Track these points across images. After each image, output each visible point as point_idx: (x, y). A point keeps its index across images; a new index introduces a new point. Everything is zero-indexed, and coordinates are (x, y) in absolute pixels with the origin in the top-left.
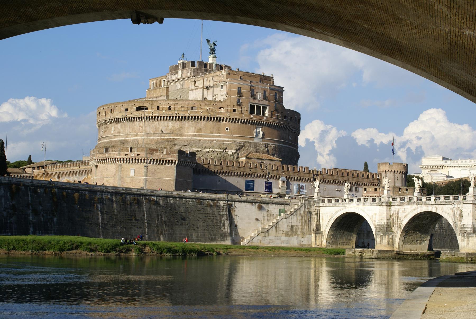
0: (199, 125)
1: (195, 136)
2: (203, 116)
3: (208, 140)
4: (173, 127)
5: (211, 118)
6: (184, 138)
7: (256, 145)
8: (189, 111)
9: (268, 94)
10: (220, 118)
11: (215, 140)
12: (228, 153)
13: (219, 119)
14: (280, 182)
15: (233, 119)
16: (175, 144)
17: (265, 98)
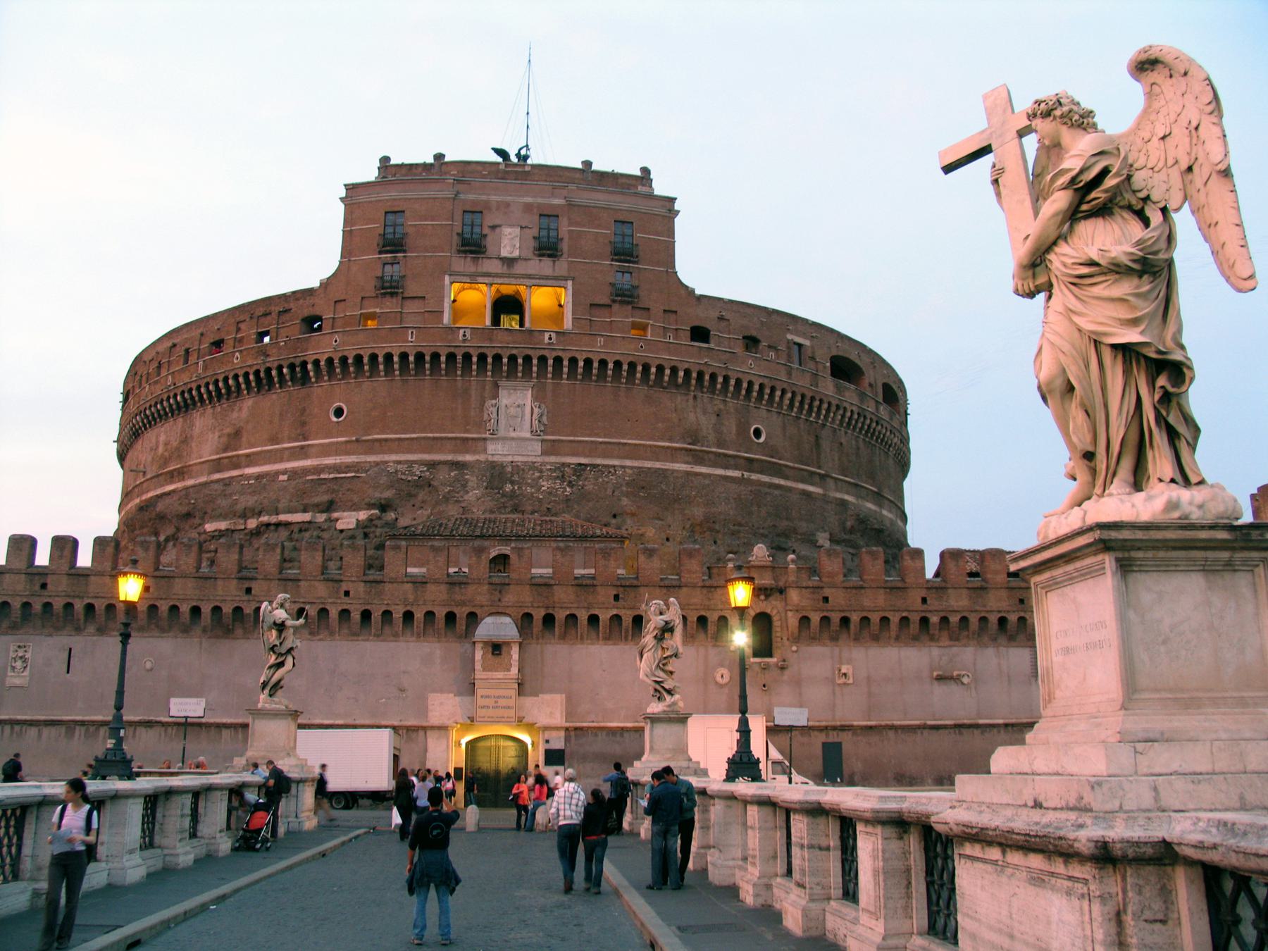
0: (235, 415)
1: (217, 466)
2: (241, 373)
3: (259, 477)
4: (166, 444)
5: (268, 370)
6: (190, 482)
7: (496, 475)
8: (201, 363)
9: (564, 228)
10: (304, 364)
11: (284, 472)
12: (340, 526)
13: (300, 374)
14: (479, 655)
15: (359, 359)
16: (162, 517)
17: (547, 248)
